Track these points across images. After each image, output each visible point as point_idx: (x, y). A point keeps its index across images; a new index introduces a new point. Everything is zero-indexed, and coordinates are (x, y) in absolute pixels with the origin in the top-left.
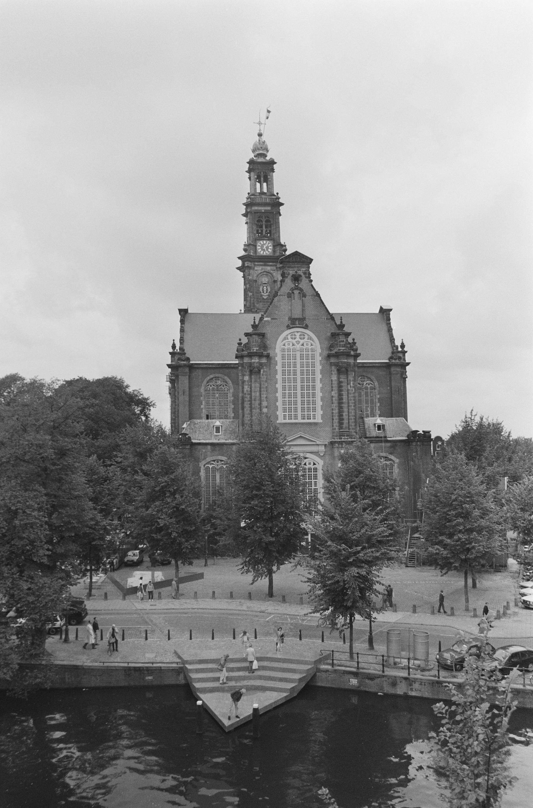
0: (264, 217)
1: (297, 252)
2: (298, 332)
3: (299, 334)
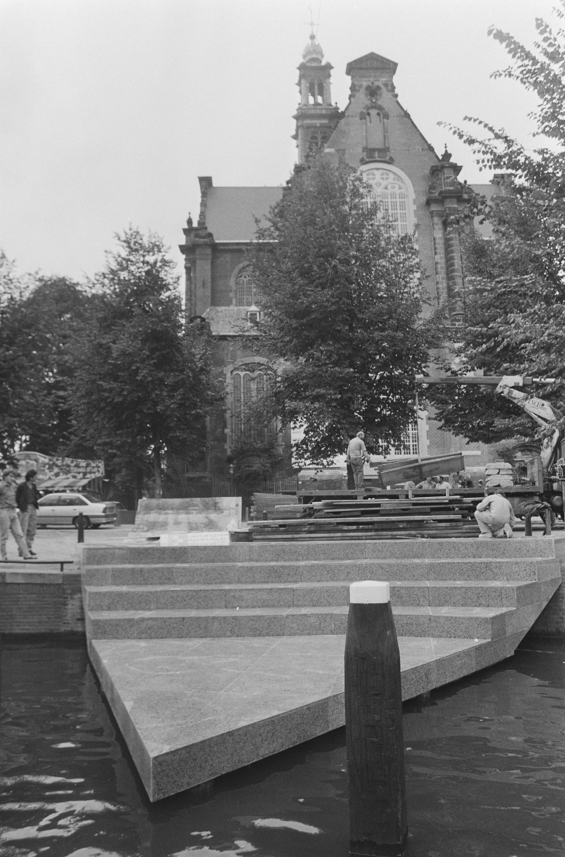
0: (319, 133)
1: (372, 54)
2: (378, 169)
3: (380, 172)
